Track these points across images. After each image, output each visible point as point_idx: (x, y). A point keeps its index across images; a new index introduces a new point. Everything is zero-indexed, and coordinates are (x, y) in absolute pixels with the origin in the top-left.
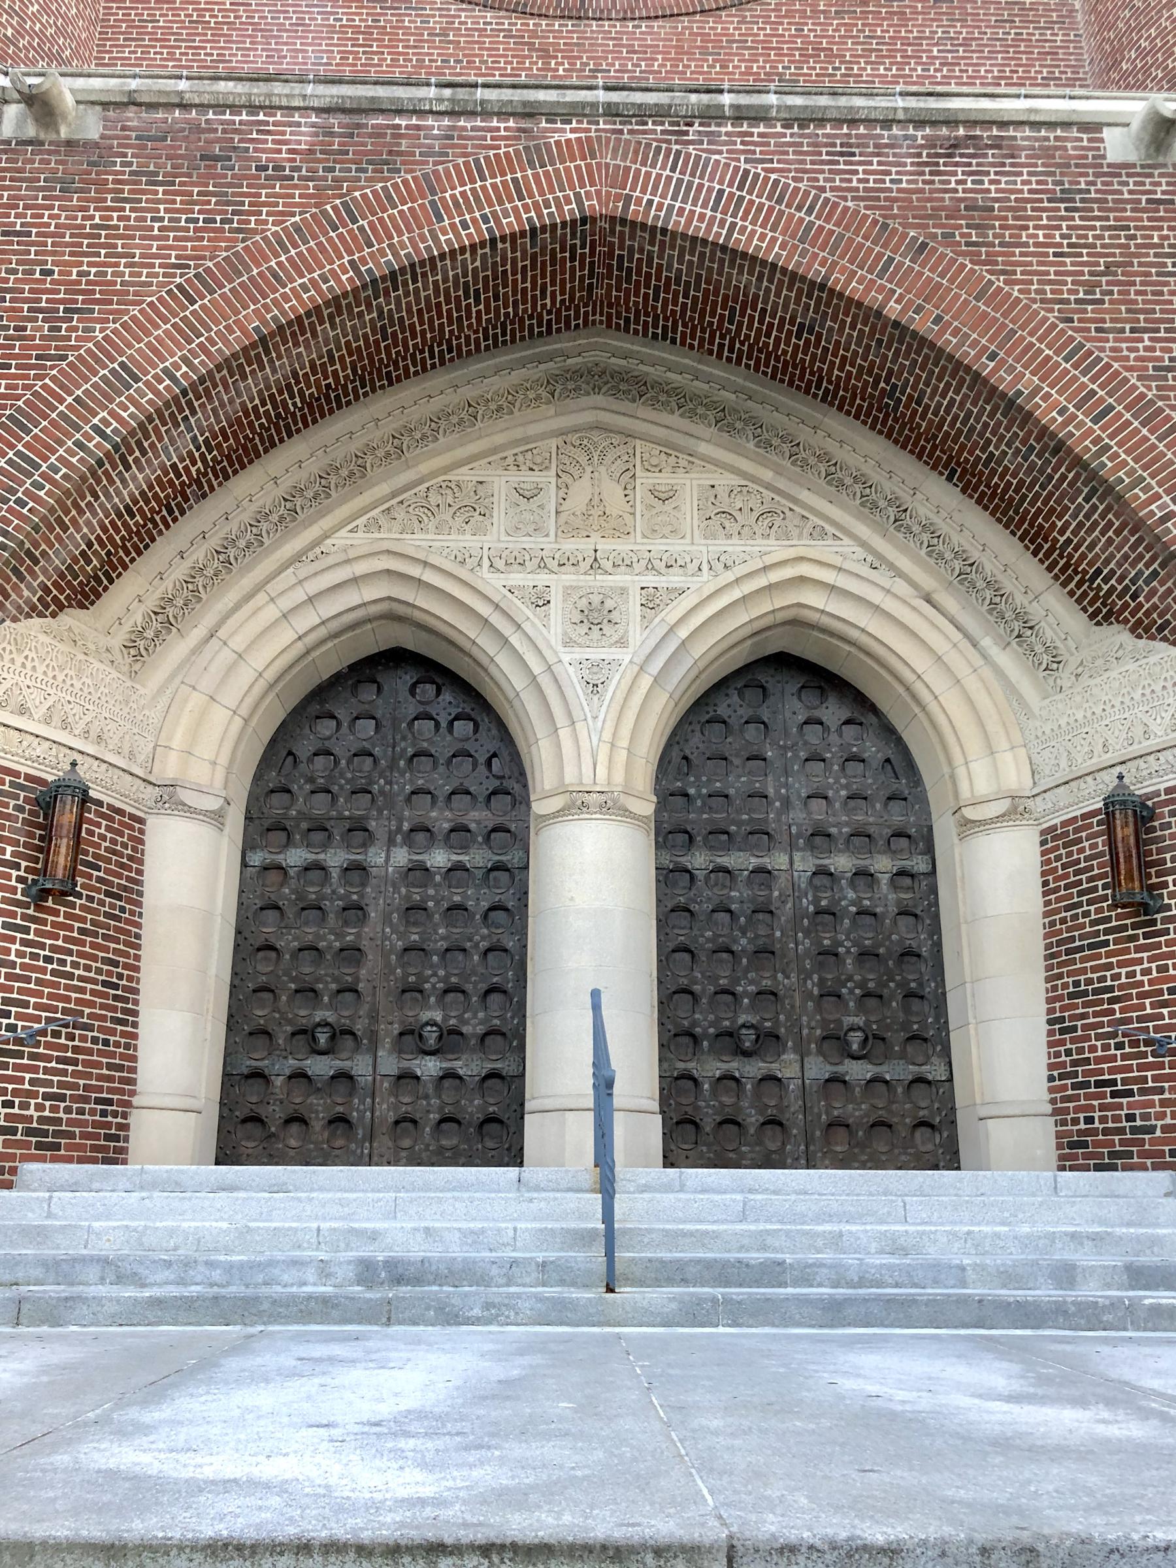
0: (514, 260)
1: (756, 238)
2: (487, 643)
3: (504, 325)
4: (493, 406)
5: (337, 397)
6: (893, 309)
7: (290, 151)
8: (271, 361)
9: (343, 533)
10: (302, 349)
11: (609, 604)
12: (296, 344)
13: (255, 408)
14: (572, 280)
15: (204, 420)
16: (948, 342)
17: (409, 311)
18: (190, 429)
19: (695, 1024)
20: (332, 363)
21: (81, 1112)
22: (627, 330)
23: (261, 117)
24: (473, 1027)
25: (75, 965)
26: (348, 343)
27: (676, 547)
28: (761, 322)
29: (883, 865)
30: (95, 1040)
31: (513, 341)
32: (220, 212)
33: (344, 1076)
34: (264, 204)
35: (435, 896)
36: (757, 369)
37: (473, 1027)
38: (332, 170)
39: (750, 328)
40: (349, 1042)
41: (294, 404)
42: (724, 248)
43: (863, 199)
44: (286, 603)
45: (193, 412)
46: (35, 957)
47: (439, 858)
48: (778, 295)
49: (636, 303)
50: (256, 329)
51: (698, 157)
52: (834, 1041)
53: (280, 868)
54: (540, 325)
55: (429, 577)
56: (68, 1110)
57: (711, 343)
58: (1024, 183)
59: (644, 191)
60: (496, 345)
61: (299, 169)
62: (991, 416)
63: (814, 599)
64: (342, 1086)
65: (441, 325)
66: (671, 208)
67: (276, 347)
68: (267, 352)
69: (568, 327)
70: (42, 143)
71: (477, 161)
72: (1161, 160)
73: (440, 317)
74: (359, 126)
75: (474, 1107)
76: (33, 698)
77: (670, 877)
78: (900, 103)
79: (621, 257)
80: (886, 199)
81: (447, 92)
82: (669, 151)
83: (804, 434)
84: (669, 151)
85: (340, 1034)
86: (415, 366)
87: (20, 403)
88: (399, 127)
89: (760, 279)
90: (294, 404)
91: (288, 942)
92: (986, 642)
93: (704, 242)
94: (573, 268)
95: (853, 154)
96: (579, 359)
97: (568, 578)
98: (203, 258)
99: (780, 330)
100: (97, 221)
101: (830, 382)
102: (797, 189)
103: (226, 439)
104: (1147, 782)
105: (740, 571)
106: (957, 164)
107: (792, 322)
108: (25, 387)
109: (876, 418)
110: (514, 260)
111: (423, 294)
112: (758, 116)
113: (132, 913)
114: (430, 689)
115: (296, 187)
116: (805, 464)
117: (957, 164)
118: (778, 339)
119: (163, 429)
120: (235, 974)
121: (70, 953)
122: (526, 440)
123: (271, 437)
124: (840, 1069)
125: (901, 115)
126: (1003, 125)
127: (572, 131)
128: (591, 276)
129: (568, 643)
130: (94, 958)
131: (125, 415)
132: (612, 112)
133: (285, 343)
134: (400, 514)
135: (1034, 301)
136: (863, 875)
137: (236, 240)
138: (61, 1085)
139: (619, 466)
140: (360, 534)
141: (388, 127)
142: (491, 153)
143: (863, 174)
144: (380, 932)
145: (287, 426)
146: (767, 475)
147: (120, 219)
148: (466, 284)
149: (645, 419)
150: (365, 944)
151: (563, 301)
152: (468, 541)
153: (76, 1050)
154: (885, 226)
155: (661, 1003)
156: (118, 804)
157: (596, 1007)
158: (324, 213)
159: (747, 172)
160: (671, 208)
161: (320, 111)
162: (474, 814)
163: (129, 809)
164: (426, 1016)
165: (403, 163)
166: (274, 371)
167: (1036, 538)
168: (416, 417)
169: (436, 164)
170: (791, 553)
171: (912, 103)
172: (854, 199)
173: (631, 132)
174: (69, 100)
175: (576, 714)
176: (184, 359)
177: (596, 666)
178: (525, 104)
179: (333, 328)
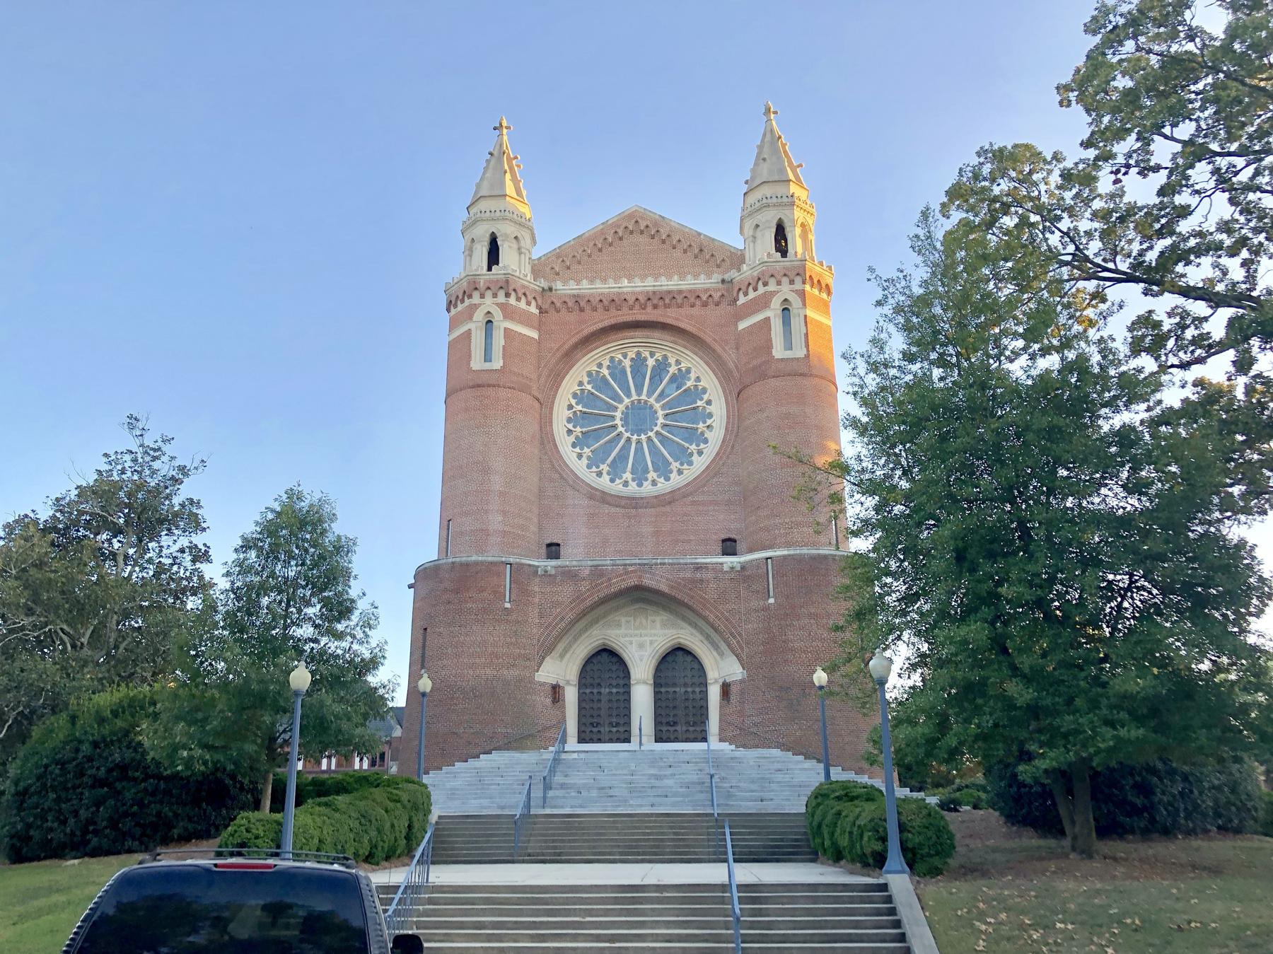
29: (698, 690)
47: (614, 690)
52: (688, 723)
63: (682, 641)
77: (656, 693)
136: (694, 692)
144: (604, 705)
152: (618, 632)
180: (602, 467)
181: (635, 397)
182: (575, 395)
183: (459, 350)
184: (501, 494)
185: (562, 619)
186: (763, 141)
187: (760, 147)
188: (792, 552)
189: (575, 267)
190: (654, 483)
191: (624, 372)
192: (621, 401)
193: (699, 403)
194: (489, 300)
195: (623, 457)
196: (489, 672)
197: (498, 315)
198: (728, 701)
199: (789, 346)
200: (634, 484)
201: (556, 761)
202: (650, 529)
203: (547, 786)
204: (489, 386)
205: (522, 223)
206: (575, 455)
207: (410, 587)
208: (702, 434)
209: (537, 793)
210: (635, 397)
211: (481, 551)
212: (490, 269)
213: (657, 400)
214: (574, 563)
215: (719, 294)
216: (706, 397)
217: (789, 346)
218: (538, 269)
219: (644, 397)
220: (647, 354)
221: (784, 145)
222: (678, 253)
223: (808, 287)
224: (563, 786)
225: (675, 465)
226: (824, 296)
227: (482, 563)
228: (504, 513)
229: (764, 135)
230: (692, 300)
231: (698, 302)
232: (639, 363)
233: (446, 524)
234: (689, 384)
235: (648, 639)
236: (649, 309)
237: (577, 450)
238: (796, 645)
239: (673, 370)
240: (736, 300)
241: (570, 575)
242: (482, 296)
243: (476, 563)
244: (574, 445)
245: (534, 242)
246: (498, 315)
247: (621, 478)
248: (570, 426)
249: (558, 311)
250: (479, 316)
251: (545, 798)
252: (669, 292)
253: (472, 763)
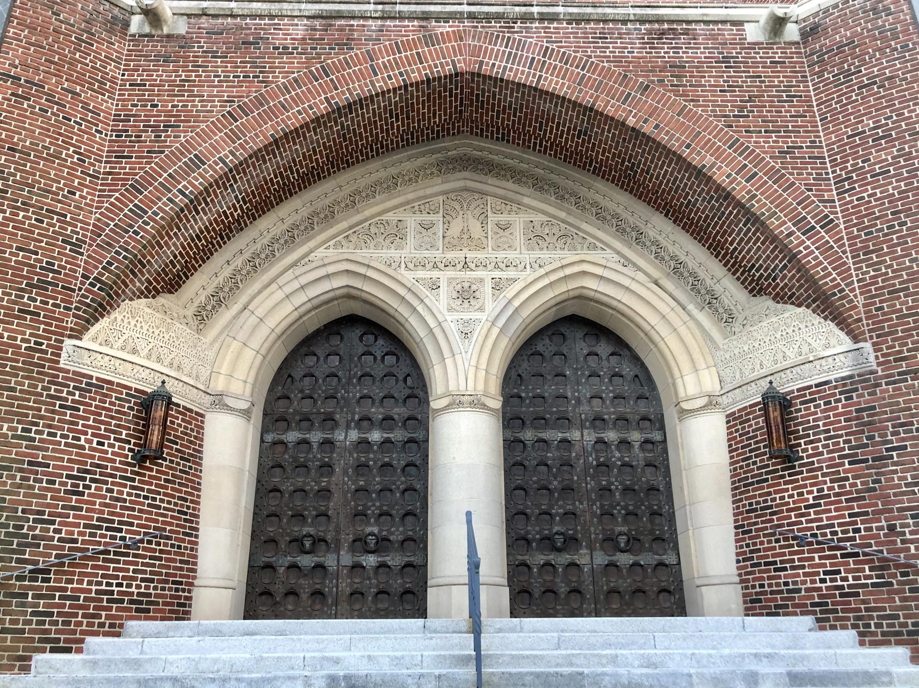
0: (418, 97)
1: (552, 83)
2: (404, 311)
3: (412, 133)
4: (406, 178)
5: (318, 174)
6: (631, 121)
7: (292, 39)
8: (280, 153)
9: (321, 249)
10: (298, 146)
11: (474, 287)
12: (295, 144)
13: (271, 180)
14: (451, 108)
15: (242, 185)
16: (663, 138)
17: (359, 126)
18: (234, 191)
19: (528, 533)
20: (315, 154)
21: (163, 589)
22: (482, 135)
23: (276, 21)
25: (162, 501)
26: (324, 143)
27: (511, 255)
28: (557, 130)
29: (636, 437)
30: (173, 546)
31: (418, 142)
32: (252, 72)
33: (320, 567)
34: (277, 67)
36: (555, 156)
37: (396, 537)
38: (316, 49)
39: (551, 133)
40: (323, 546)
41: (294, 177)
42: (536, 89)
43: (612, 62)
44: (288, 289)
45: (236, 182)
46: (138, 496)
47: (376, 436)
48: (566, 114)
49: (487, 120)
50: (272, 135)
51: (520, 41)
52: (610, 542)
53: (282, 442)
54: (433, 133)
55: (370, 273)
56: (155, 588)
57: (530, 142)
58: (701, 54)
59: (490, 58)
60: (408, 145)
61: (296, 48)
62: (689, 179)
63: (591, 284)
64: (319, 572)
65: (377, 134)
66: (505, 67)
67: (283, 144)
68: (278, 148)
69: (448, 134)
70: (153, 36)
71: (396, 43)
72: (777, 40)
73: (376, 128)
74: (331, 25)
75: (397, 584)
76: (141, 345)
77: (511, 445)
78: (632, 11)
79: (478, 95)
80: (626, 62)
81: (380, 7)
82: (504, 37)
83: (583, 191)
84: (504, 37)
85: (317, 541)
86: (362, 156)
87: (137, 177)
88: (353, 25)
89: (556, 106)
90: (294, 177)
91: (287, 487)
92: (691, 307)
93: (524, 85)
94: (451, 101)
95: (606, 38)
96: (455, 152)
97: (451, 273)
98: (243, 97)
99: (568, 134)
100: (183, 77)
101: (597, 163)
102: (576, 57)
103: (254, 197)
104: (788, 385)
105: (548, 268)
106: (664, 43)
107: (575, 130)
108: (140, 169)
109: (624, 182)
110: (418, 97)
111: (366, 116)
112: (553, 18)
113: (196, 470)
114: (371, 338)
115: (295, 58)
116: (584, 208)
117: (664, 43)
118: (567, 139)
119: (218, 191)
120: (256, 506)
121: (159, 493)
122: (425, 197)
123: (280, 196)
124: (614, 558)
125: (632, 18)
126: (689, 22)
127: (450, 27)
128: (461, 105)
129: (450, 309)
130: (173, 497)
131: (197, 183)
132: (472, 16)
133: (288, 142)
134: (354, 238)
135: (710, 116)
136: (625, 443)
137: (261, 87)
138: (152, 573)
139: (478, 211)
140: (331, 250)
141: (347, 25)
142: (405, 39)
144: (341, 480)
145: (289, 190)
146: (563, 215)
147: (196, 76)
148: (391, 110)
149: (492, 184)
150: (333, 488)
151: (445, 120)
152: (393, 253)
153: (161, 551)
154: (625, 76)
155: (507, 520)
156: (189, 406)
157: (469, 522)
158: (311, 72)
159: (547, 48)
160: (505, 67)
161: (308, 17)
162: (396, 410)
163: (195, 409)
164: (369, 529)
165: (355, 44)
166: (282, 159)
167: (717, 248)
168: (363, 184)
169: (373, 45)
170: (577, 258)
171: (638, 11)
172: (607, 62)
173: (482, 27)
174: (169, 13)
175: (456, 350)
176: (231, 152)
177: (467, 322)
178: (423, 12)
179: (316, 134)
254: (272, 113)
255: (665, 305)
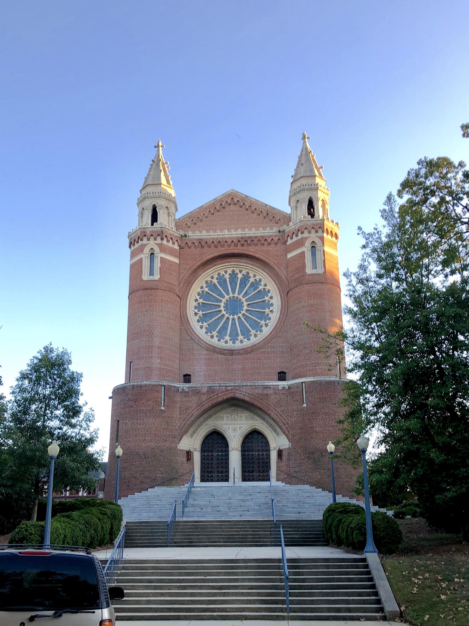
2: (224, 433)
6: (259, 405)
24: (224, 471)
27: (242, 422)
29: (265, 453)
35: (220, 458)
37: (224, 471)
47: (220, 454)
52: (259, 471)
63: (257, 427)
75: (224, 478)
77: (243, 455)
85: (211, 472)
91: (206, 463)
97: (232, 426)
112: (247, 386)
136: (262, 454)
143: (257, 391)
144: (215, 462)
152: (222, 422)
180: (213, 333)
181: (231, 295)
182: (199, 294)
183: (136, 269)
184: (159, 347)
185: (191, 416)
186: (301, 154)
187: (300, 158)
188: (316, 379)
189: (199, 224)
190: (242, 342)
191: (225, 281)
192: (224, 297)
193: (266, 298)
194: (152, 241)
195: (224, 328)
196: (153, 444)
197: (157, 250)
198: (281, 459)
199: (315, 267)
200: (231, 342)
201: (189, 492)
202: (240, 367)
203: (184, 505)
204: (152, 289)
205: (169, 199)
206: (199, 327)
207: (110, 398)
208: (268, 315)
209: (179, 509)
210: (231, 295)
211: (148, 378)
212: (152, 225)
213: (244, 297)
214: (199, 385)
215: (277, 238)
216: (270, 295)
217: (315, 267)
218: (179, 225)
219: (236, 295)
220: (238, 271)
221: (313, 156)
222: (255, 215)
223: (325, 235)
224: (193, 505)
225: (253, 332)
226: (334, 239)
227: (149, 385)
228: (161, 358)
229: (302, 151)
230: (263, 242)
231: (266, 243)
232: (233, 276)
233: (129, 364)
234: (261, 288)
235: (238, 426)
236: (239, 247)
237: (200, 324)
238: (318, 429)
239: (252, 280)
240: (286, 241)
241: (196, 392)
242: (148, 239)
243: (146, 386)
244: (198, 321)
245: (177, 210)
246: (157, 250)
247: (224, 339)
248: (196, 311)
249: (190, 248)
250: (147, 251)
251: (183, 512)
252: (250, 237)
253: (144, 493)
254: (203, 406)
255: (268, 431)
